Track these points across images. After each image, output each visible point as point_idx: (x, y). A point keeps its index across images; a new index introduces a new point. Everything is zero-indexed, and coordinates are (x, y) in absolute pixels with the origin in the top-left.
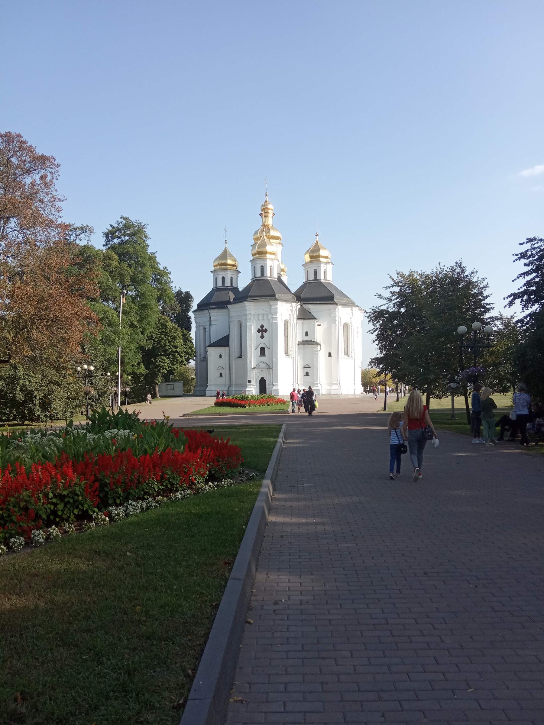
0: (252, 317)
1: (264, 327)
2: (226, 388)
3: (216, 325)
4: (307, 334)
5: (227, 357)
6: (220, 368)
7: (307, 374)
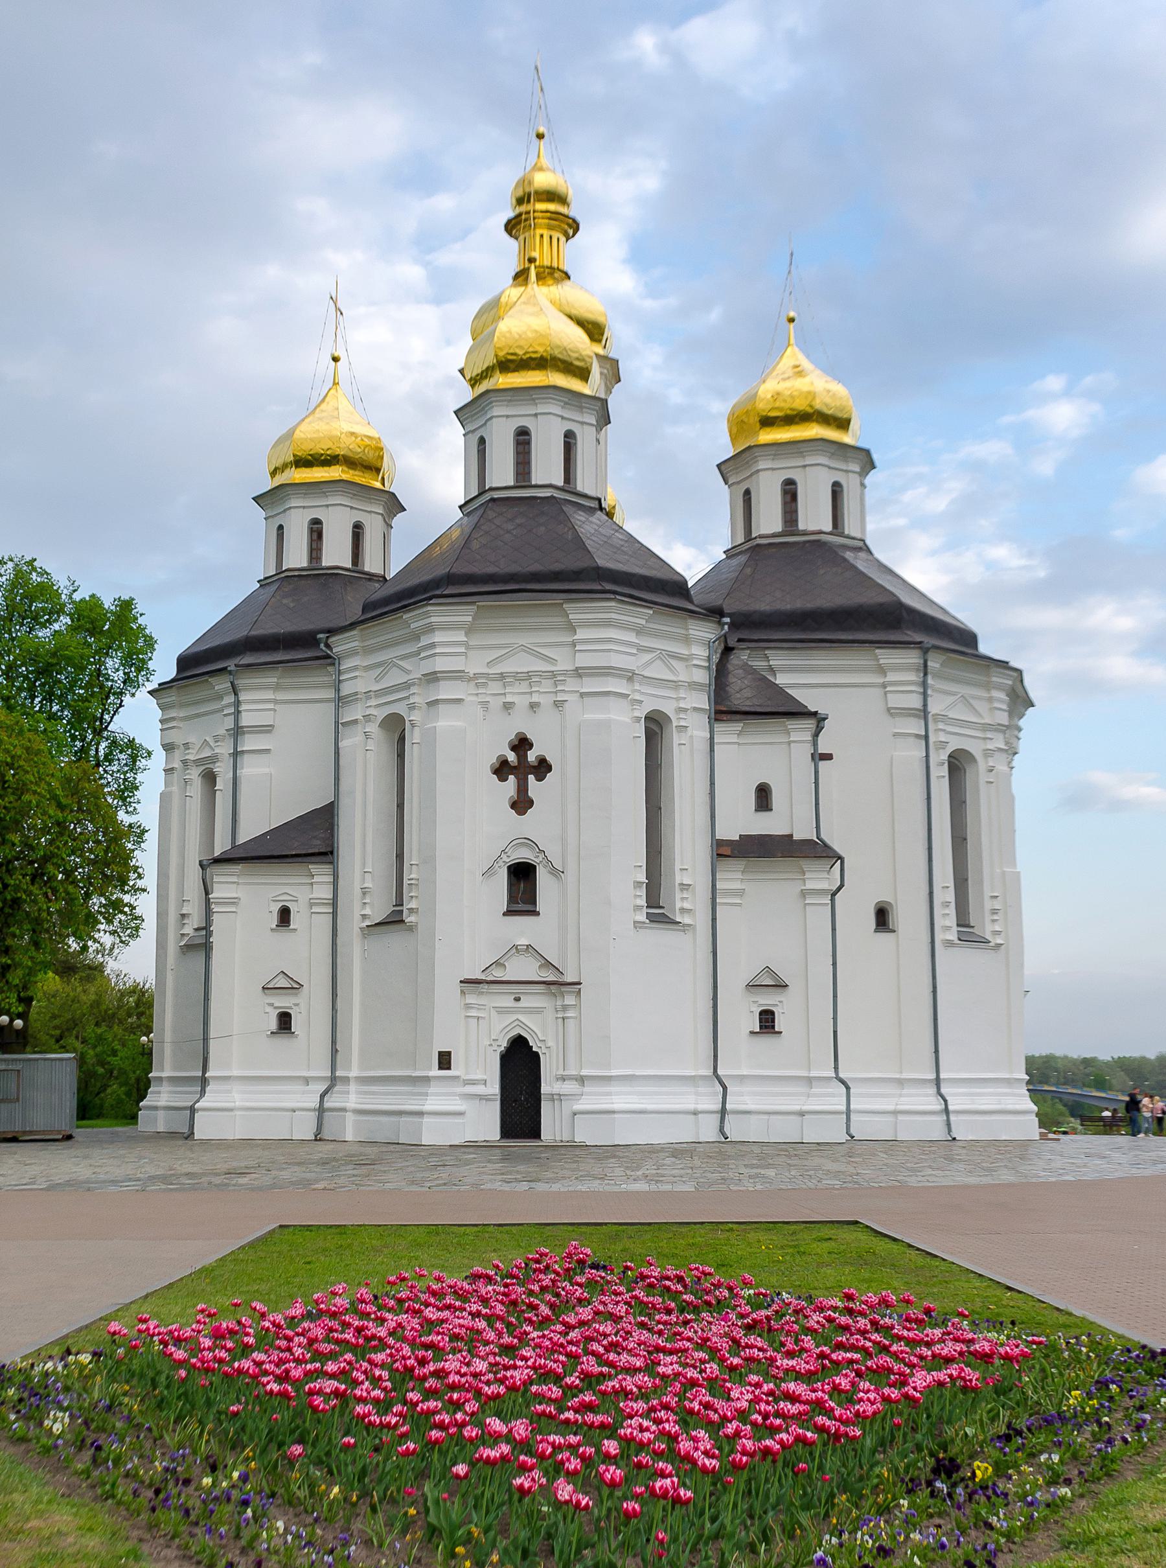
1: (531, 746)
3: (267, 751)
6: (282, 982)
7: (767, 1020)
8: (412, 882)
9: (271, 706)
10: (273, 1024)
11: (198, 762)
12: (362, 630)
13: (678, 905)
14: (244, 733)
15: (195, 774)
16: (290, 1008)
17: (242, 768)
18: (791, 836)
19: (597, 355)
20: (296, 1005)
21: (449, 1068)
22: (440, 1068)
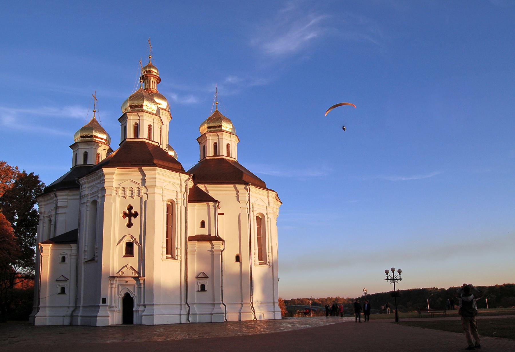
0: (114, 193)
2: (69, 312)
4: (203, 224)
5: (74, 261)
6: (62, 278)
8: (97, 248)
9: (66, 200)
10: (59, 291)
11: (48, 217)
12: (87, 177)
13: (176, 254)
14: (58, 208)
15: (47, 220)
16: (64, 286)
17: (58, 218)
18: (210, 235)
19: (160, 104)
20: (67, 285)
21: (105, 303)
22: (103, 303)
